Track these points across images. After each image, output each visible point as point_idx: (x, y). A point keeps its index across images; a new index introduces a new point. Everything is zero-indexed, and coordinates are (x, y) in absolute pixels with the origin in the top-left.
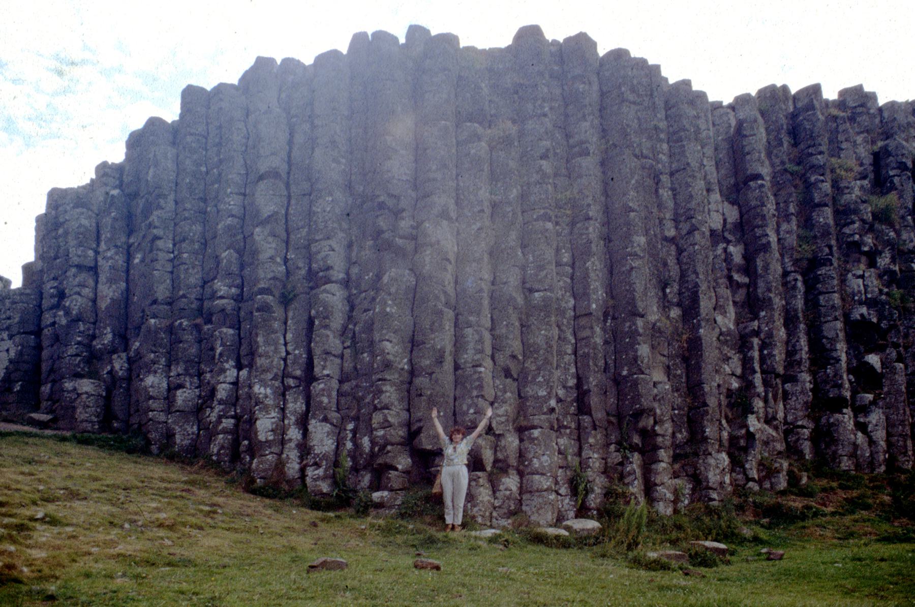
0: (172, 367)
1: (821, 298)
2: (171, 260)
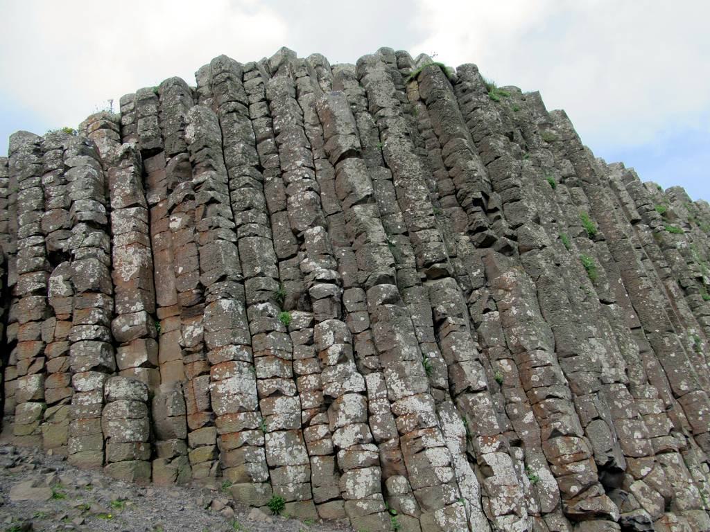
0: (259, 365)
2: (235, 230)
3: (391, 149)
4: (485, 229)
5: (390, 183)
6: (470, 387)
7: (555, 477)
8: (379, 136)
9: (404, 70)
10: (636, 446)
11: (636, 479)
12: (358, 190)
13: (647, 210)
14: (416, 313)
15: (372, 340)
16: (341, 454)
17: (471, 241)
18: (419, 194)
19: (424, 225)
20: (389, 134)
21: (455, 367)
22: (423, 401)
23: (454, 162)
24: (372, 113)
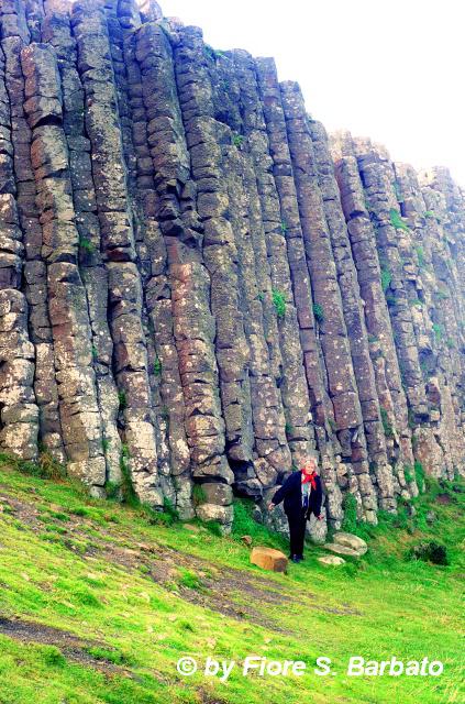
1: (403, 324)
3: (94, 118)
4: (174, 218)
5: (87, 155)
6: (129, 366)
7: (189, 447)
8: (85, 100)
9: (123, 19)
10: (267, 430)
11: (260, 456)
12: (54, 162)
13: (379, 200)
14: (93, 296)
15: (48, 313)
16: (5, 409)
17: (160, 227)
18: (115, 172)
19: (115, 207)
20: (94, 101)
21: (120, 346)
22: (83, 371)
23: (157, 142)
24: (81, 72)
